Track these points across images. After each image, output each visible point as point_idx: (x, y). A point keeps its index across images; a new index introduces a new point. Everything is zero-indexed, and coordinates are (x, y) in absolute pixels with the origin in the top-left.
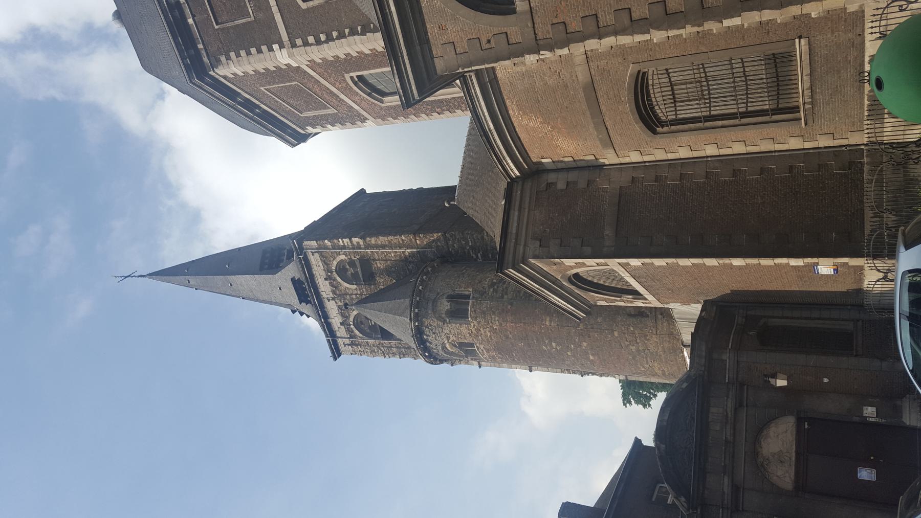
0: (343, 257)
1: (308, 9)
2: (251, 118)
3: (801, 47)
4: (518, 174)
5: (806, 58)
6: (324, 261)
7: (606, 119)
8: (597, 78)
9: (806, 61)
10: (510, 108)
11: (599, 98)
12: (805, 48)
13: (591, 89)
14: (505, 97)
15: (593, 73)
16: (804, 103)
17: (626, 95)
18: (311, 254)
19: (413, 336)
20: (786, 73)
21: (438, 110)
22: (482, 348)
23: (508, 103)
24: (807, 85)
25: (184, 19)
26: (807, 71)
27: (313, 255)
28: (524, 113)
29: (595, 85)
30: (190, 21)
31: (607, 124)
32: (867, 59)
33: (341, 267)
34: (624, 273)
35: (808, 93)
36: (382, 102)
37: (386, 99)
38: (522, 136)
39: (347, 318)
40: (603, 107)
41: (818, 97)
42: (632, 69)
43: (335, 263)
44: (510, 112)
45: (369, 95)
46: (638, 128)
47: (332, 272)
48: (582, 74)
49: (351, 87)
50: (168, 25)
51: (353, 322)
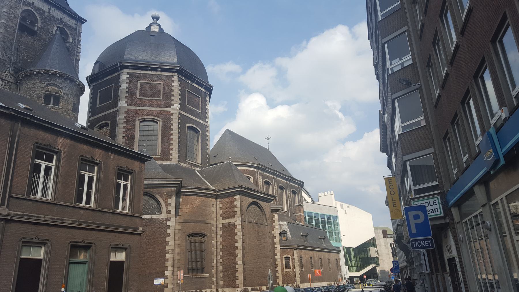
0: (71, 40)
1: (186, 126)
2: (149, 64)
3: (207, 275)
4: (182, 190)
5: (205, 276)
6: (70, 27)
7: (195, 224)
8: (206, 225)
9: (204, 276)
10: (202, 198)
11: (202, 224)
12: (207, 276)
13: (205, 223)
14: (205, 198)
15: (208, 224)
16: (193, 276)
17: (201, 231)
18: (76, 23)
19: (73, 77)
20: (192, 272)
21: (126, 138)
22: (59, 111)
23: (204, 198)
24: (198, 277)
25: (191, 81)
26: (201, 277)
27: (75, 24)
28: (200, 201)
29: (205, 224)
30: (189, 82)
31: (193, 224)
32: (202, 290)
33: (63, 32)
34: (158, 216)
35: (196, 277)
36: (138, 120)
37: (139, 122)
38: (193, 197)
39: (36, 11)
40: (199, 224)
41: (194, 279)
42: (208, 234)
43: (68, 33)
44: (201, 197)
45: (145, 119)
46: (191, 232)
47: (63, 25)
48: (208, 221)
49: (153, 116)
50: (193, 75)
51: (32, 11)
